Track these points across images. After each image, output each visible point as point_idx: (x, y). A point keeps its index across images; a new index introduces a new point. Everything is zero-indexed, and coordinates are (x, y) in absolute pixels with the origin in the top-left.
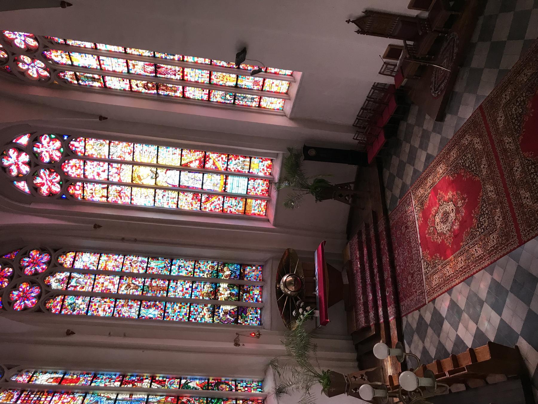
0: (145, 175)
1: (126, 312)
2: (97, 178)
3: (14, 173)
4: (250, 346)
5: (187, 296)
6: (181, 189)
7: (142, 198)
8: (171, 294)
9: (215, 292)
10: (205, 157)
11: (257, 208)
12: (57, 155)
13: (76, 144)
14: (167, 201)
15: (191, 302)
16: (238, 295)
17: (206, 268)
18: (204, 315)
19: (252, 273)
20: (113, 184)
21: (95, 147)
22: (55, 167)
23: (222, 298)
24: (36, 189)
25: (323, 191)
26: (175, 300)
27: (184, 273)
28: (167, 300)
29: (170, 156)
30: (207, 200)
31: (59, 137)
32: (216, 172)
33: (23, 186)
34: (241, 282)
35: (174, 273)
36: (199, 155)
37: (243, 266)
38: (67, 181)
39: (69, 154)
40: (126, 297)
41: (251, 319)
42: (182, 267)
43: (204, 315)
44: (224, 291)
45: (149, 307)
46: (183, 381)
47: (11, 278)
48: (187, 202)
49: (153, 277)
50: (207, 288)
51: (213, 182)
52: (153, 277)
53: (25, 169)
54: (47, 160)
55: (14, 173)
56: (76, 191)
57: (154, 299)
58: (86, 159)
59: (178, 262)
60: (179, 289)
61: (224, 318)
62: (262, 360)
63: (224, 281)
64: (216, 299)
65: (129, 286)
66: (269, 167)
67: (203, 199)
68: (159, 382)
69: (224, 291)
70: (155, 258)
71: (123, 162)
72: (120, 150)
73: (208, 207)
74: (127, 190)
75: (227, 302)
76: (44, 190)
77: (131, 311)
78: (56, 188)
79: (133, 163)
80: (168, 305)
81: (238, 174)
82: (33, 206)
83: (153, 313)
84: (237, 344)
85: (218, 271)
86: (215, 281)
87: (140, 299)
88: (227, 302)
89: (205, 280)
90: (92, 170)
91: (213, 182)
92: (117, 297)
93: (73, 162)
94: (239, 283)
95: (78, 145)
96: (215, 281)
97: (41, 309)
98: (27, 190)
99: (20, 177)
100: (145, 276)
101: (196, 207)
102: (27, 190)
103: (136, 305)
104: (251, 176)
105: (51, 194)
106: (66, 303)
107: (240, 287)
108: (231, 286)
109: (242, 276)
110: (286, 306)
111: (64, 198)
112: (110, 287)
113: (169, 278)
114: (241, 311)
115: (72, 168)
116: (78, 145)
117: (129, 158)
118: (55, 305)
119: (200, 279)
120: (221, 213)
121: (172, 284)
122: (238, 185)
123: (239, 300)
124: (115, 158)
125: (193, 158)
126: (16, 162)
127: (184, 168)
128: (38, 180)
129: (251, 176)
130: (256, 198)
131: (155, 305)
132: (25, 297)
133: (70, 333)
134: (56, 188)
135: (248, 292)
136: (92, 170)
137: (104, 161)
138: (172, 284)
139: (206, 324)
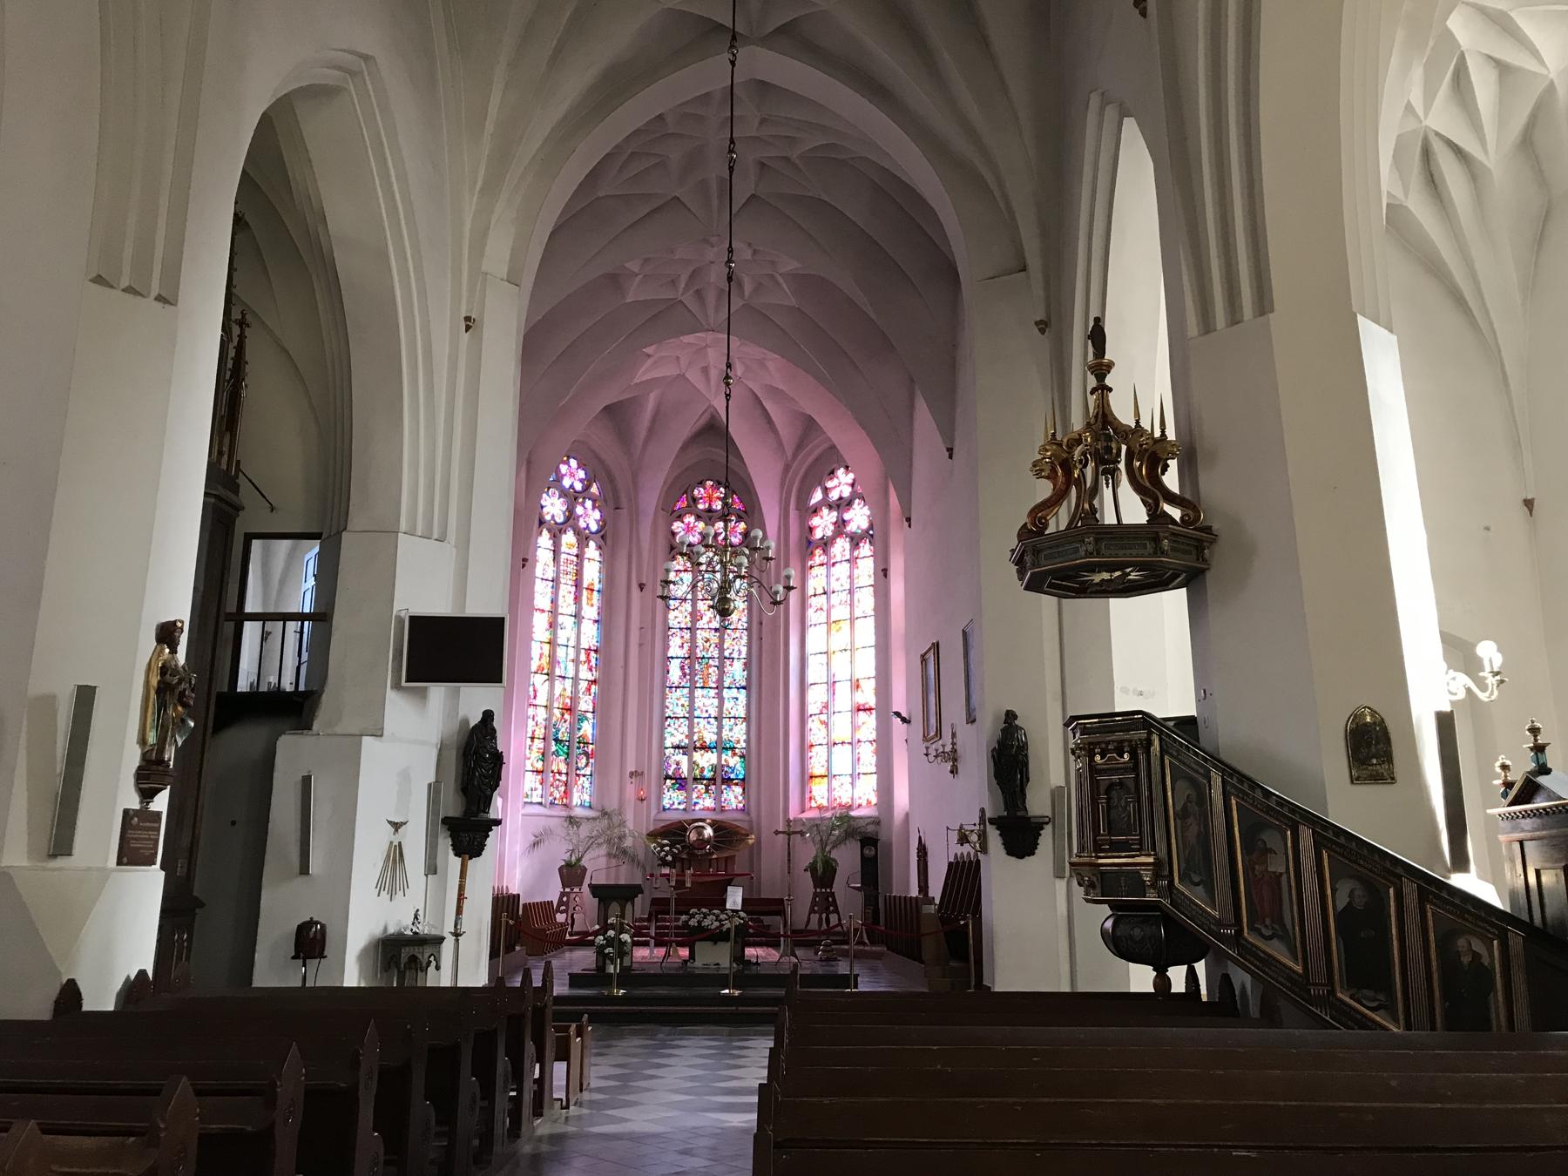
0: (841, 638)
1: (675, 642)
2: (833, 580)
3: (829, 484)
4: (630, 790)
5: (697, 713)
6: (832, 685)
7: (816, 639)
8: (698, 693)
9: (705, 748)
10: (870, 709)
11: (819, 791)
12: (851, 528)
13: (867, 545)
14: (815, 672)
15: (690, 718)
16: (703, 778)
17: (737, 733)
18: (676, 734)
19: (733, 797)
20: (828, 600)
21: (866, 567)
22: (841, 525)
23: (697, 756)
24: (816, 511)
25: (824, 874)
26: (692, 698)
27: (728, 705)
28: (693, 688)
29: (867, 664)
30: (822, 723)
31: (871, 527)
32: (855, 728)
33: (818, 496)
34: (719, 781)
35: (726, 693)
36: (872, 702)
37: (743, 782)
38: (826, 544)
39: (855, 541)
40: (693, 639)
41: (673, 798)
42: (737, 703)
43: (676, 734)
44: (706, 760)
45: (682, 668)
46: (590, 715)
47: (710, 510)
48: (816, 697)
49: (721, 668)
50: (710, 738)
51: (841, 729)
52: (721, 668)
53: (834, 495)
54: (847, 516)
55: (829, 484)
56: (819, 557)
57: (693, 674)
58: (852, 561)
59: (742, 695)
60: (706, 701)
61: (672, 761)
62: (612, 805)
63: (719, 758)
64: (695, 749)
65: (707, 641)
66: (869, 802)
67: (824, 717)
68: (589, 689)
69: (706, 760)
70: (747, 666)
71: (852, 605)
72: (866, 601)
73: (814, 725)
74: (822, 617)
75: (692, 764)
76: (815, 521)
77: (676, 648)
78: (818, 534)
79: (852, 620)
80: (686, 691)
81: (856, 760)
82: (793, 513)
83: (675, 674)
84: (632, 774)
85: (733, 749)
86: (721, 746)
87: (691, 657)
88: (692, 764)
89: (719, 733)
90: (842, 570)
91: (841, 729)
92: (692, 629)
93: (847, 546)
94: (721, 778)
95: (866, 549)
96: (721, 746)
97: (673, 550)
98: (813, 502)
99: (826, 491)
100: (722, 658)
101: (812, 708)
102: (813, 502)
103: (683, 652)
104: (854, 776)
105: (811, 529)
106: (682, 575)
107: (713, 780)
108: (714, 768)
109: (728, 781)
110: (674, 832)
111: (810, 545)
112: (706, 619)
113: (720, 687)
114: (681, 783)
115: (841, 547)
116: (866, 549)
117: (857, 613)
118: (680, 563)
119: (720, 727)
120: (807, 744)
121: (712, 693)
122: (842, 760)
123: (695, 779)
124: (856, 596)
125: (868, 696)
126: (841, 484)
127: (856, 686)
128: (825, 511)
129: (854, 776)
130: (830, 790)
131: (685, 675)
132: (689, 530)
133: (641, 587)
134: (818, 534)
135: (707, 791)
136: (842, 570)
137: (852, 583)
138: (712, 693)
139: (662, 739)
